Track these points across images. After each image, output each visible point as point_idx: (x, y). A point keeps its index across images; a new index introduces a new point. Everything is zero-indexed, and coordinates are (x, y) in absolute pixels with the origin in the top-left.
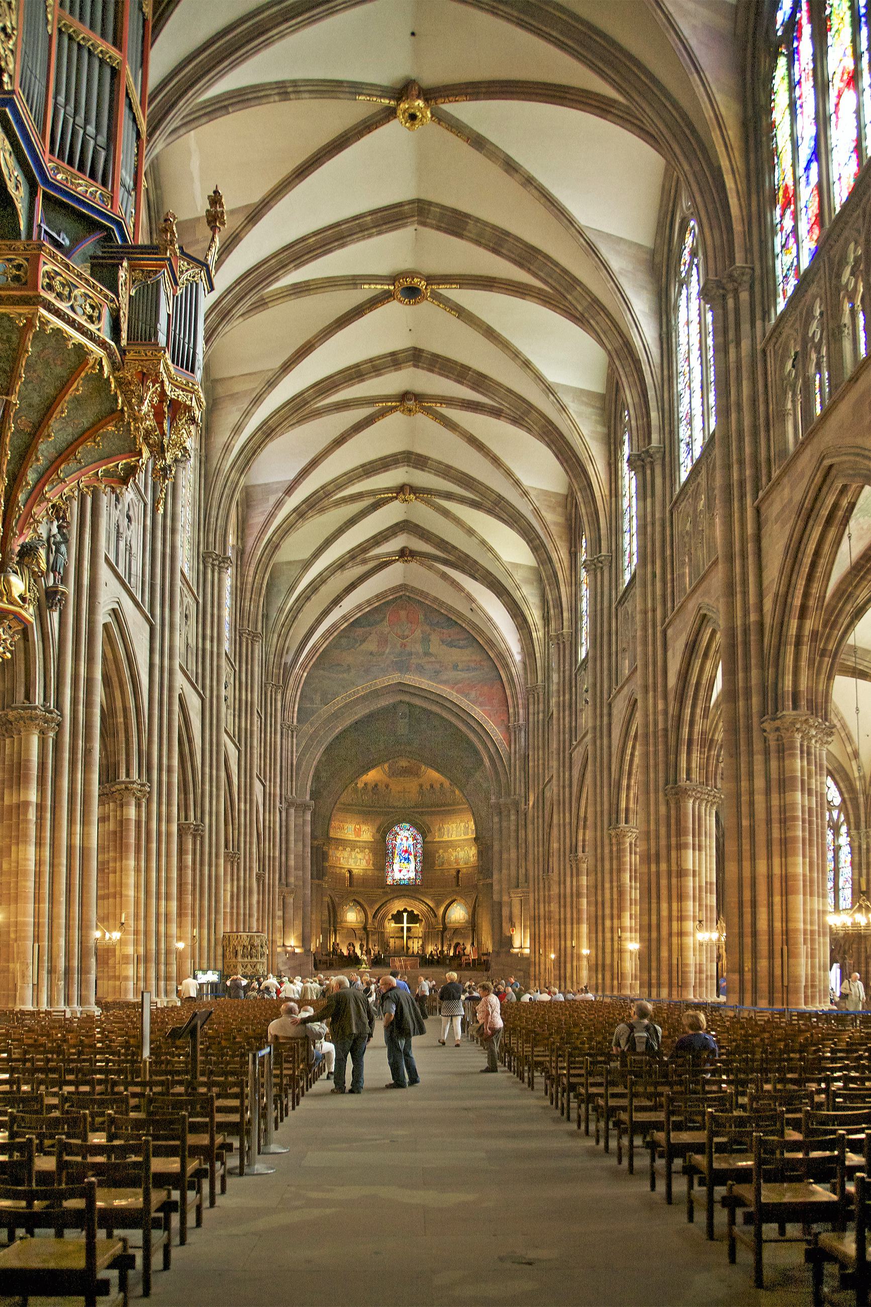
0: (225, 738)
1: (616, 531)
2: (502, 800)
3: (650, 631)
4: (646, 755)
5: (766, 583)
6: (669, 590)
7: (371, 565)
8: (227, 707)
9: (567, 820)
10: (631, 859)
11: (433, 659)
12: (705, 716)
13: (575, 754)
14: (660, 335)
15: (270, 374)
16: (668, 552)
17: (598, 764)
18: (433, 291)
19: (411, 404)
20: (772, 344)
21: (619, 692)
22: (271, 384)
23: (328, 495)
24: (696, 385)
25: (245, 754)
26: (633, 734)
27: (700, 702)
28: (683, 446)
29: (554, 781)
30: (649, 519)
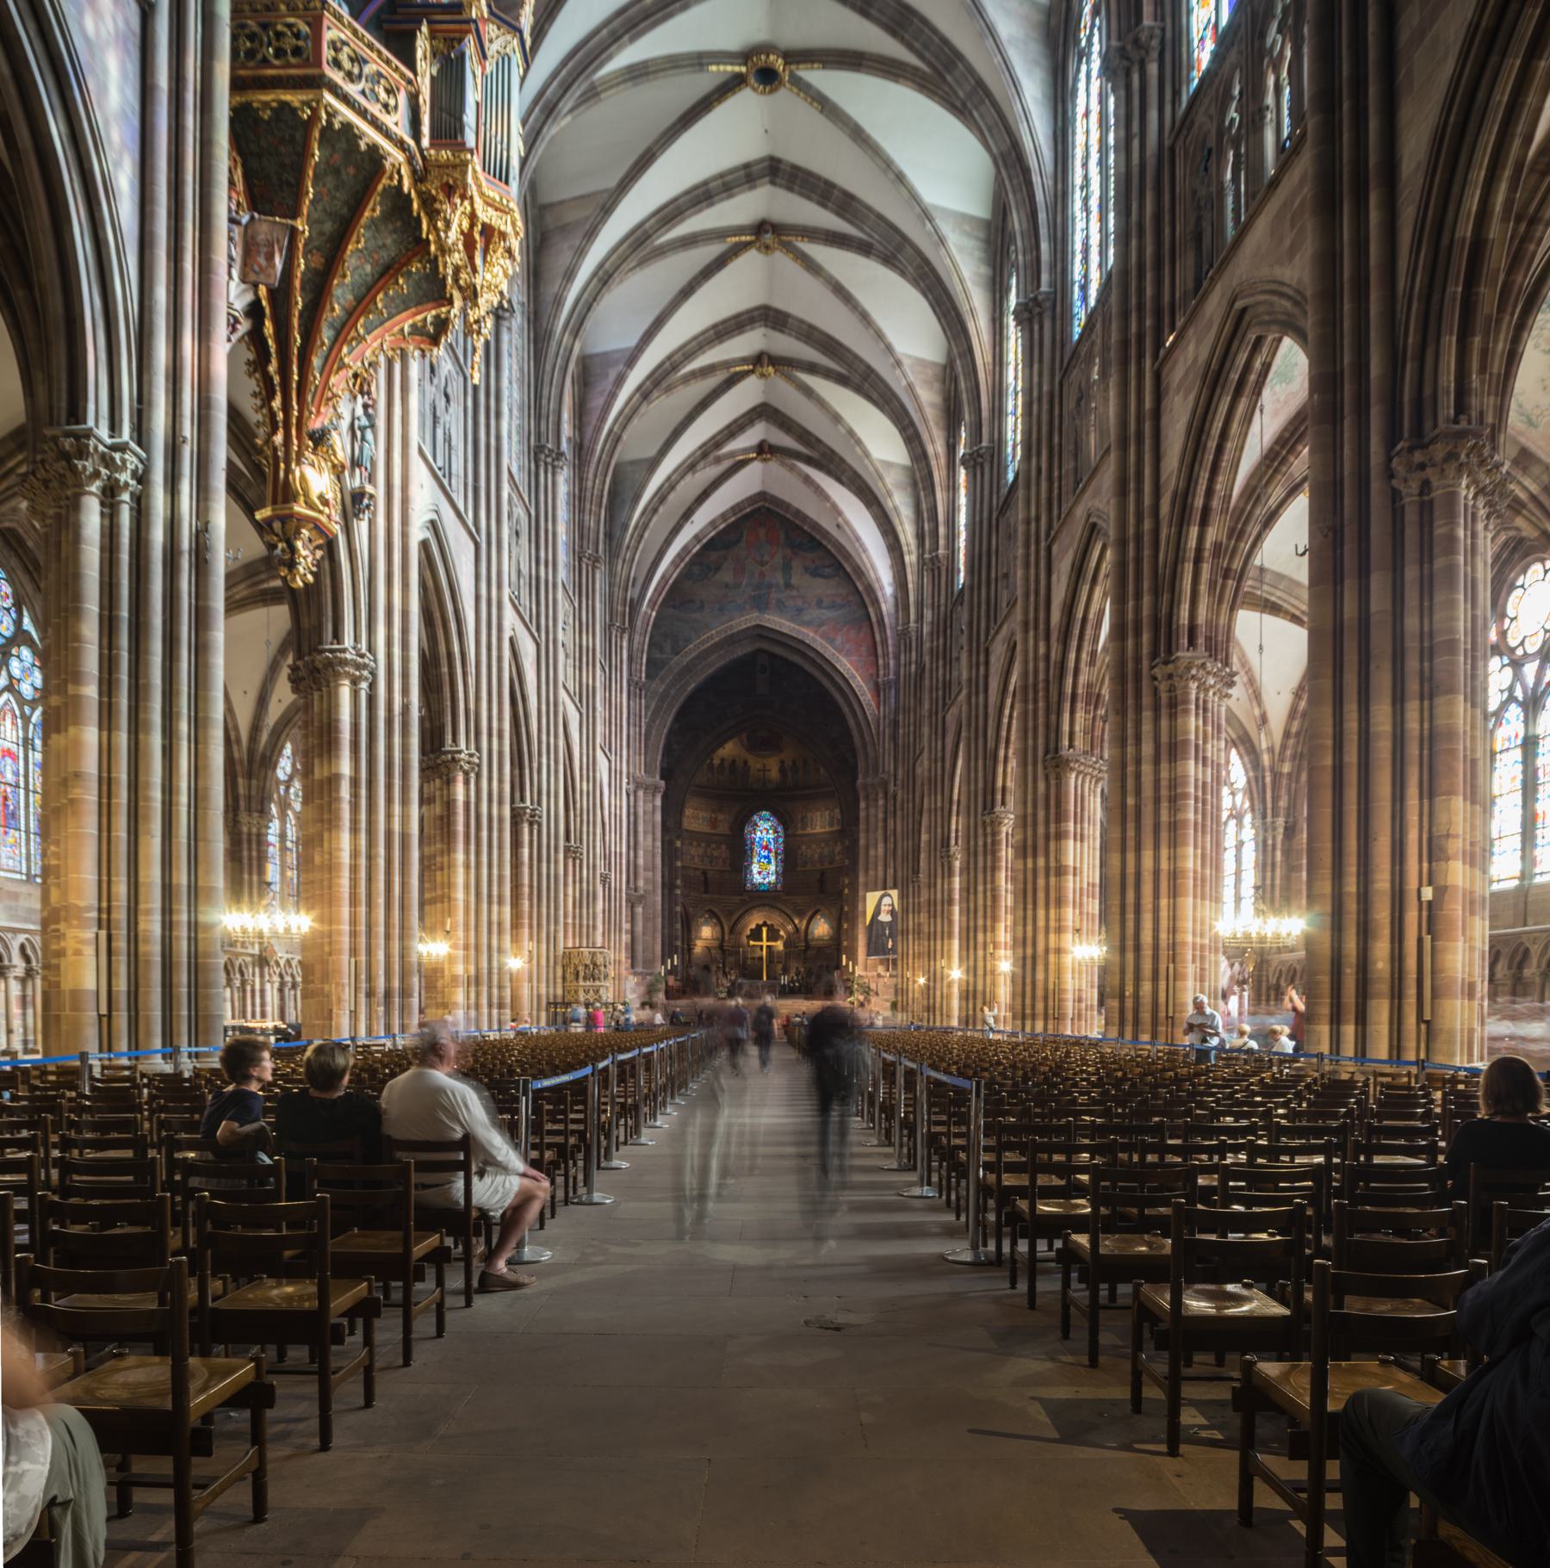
1: (998, 412)
2: (869, 780)
3: (1033, 548)
4: (1024, 716)
5: (1163, 478)
6: (1056, 492)
7: (726, 464)
8: (567, 656)
10: (1006, 854)
11: (794, 593)
12: (1092, 663)
13: (949, 716)
14: (1055, 133)
15: (605, 195)
18: (792, 75)
19: (768, 238)
20: (1182, 138)
21: (997, 632)
22: (607, 210)
23: (675, 367)
24: (1094, 203)
25: (588, 721)
26: (1011, 688)
27: (1086, 644)
28: (1076, 288)
29: (926, 754)
30: (1035, 394)
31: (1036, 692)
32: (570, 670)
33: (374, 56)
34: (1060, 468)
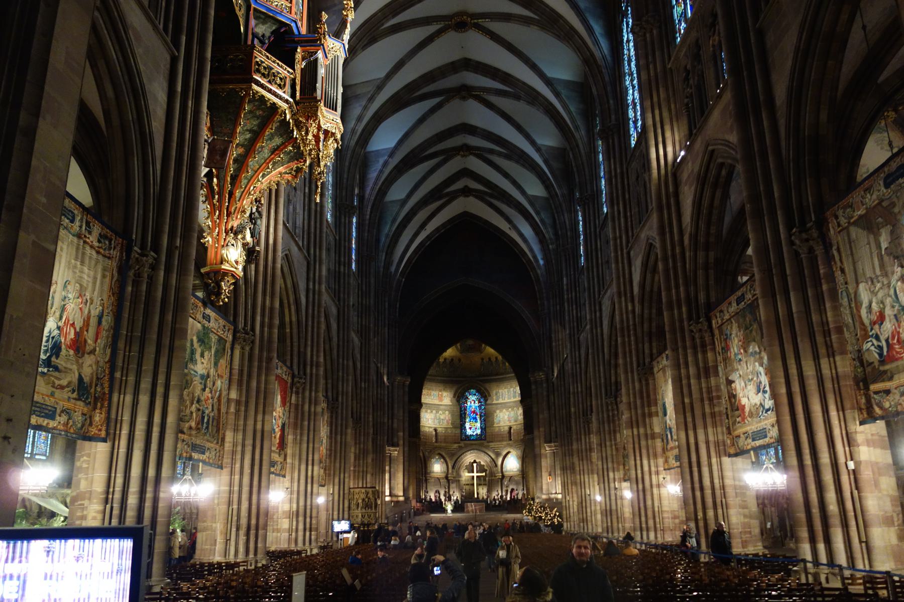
3: (619, 253)
9: (579, 389)
17: (595, 349)
21: (605, 293)
32: (355, 319)
33: (276, 65)
34: (631, 212)
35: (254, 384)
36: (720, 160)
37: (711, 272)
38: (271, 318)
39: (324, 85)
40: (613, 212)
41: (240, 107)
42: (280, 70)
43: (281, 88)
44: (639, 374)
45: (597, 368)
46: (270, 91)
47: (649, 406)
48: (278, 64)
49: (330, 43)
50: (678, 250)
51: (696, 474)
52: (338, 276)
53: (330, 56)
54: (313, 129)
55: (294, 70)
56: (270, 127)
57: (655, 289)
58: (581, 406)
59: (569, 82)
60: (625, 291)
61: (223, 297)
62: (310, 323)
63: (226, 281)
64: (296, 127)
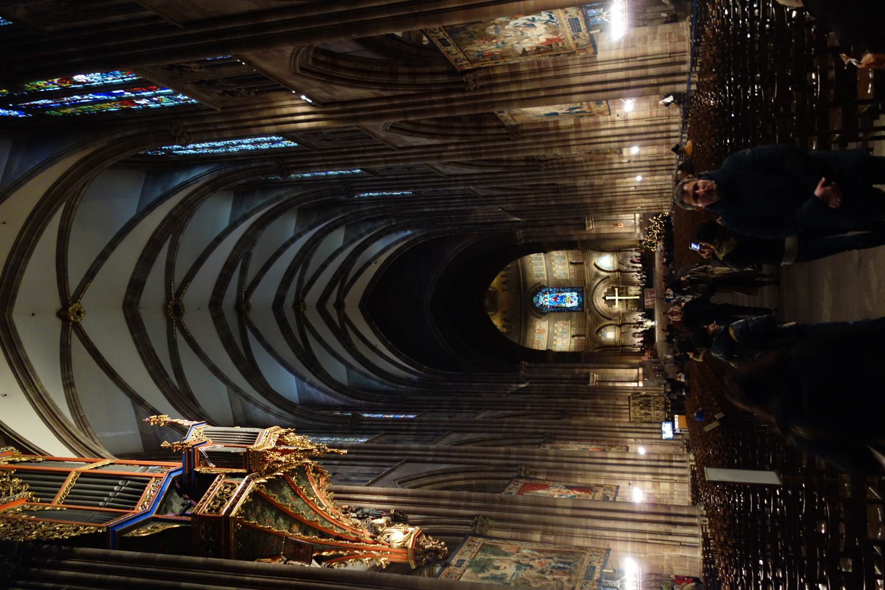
0: (478, 418)
3: (399, 158)
6: (371, 148)
9: (533, 196)
16: (345, 150)
17: (492, 181)
21: (439, 171)
31: (475, 149)
32: (464, 415)
34: (360, 146)
35: (526, 516)
36: (310, 61)
37: (418, 70)
38: (461, 499)
39: (232, 445)
40: (360, 164)
41: (253, 528)
42: (217, 488)
43: (235, 488)
44: (518, 139)
45: (512, 179)
46: (237, 499)
47: (548, 129)
48: (211, 490)
49: (191, 439)
50: (397, 102)
51: (614, 85)
52: (420, 431)
53: (205, 439)
54: (275, 456)
55: (218, 474)
56: (272, 498)
57: (435, 123)
58: (549, 195)
59: (233, 206)
60: (437, 152)
61: (439, 547)
62: (466, 460)
63: (424, 543)
64: (273, 472)
